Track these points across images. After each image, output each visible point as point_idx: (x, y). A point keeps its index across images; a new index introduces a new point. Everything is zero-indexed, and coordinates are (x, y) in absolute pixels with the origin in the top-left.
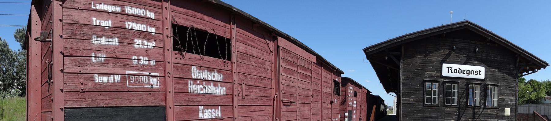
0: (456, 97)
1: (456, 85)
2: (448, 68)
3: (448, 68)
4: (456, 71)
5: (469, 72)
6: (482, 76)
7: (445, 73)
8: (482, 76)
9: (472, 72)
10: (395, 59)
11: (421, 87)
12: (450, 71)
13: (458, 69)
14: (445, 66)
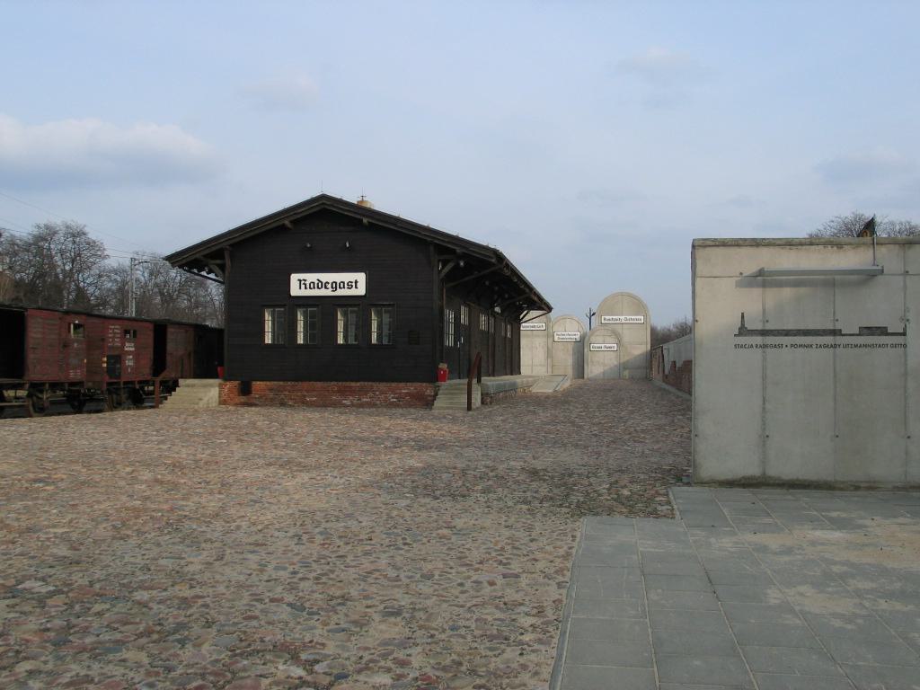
2: (300, 281)
3: (300, 281)
4: (312, 286)
5: (335, 286)
6: (361, 290)
7: (295, 291)
8: (361, 290)
9: (342, 285)
13: (316, 282)
14: (295, 278)
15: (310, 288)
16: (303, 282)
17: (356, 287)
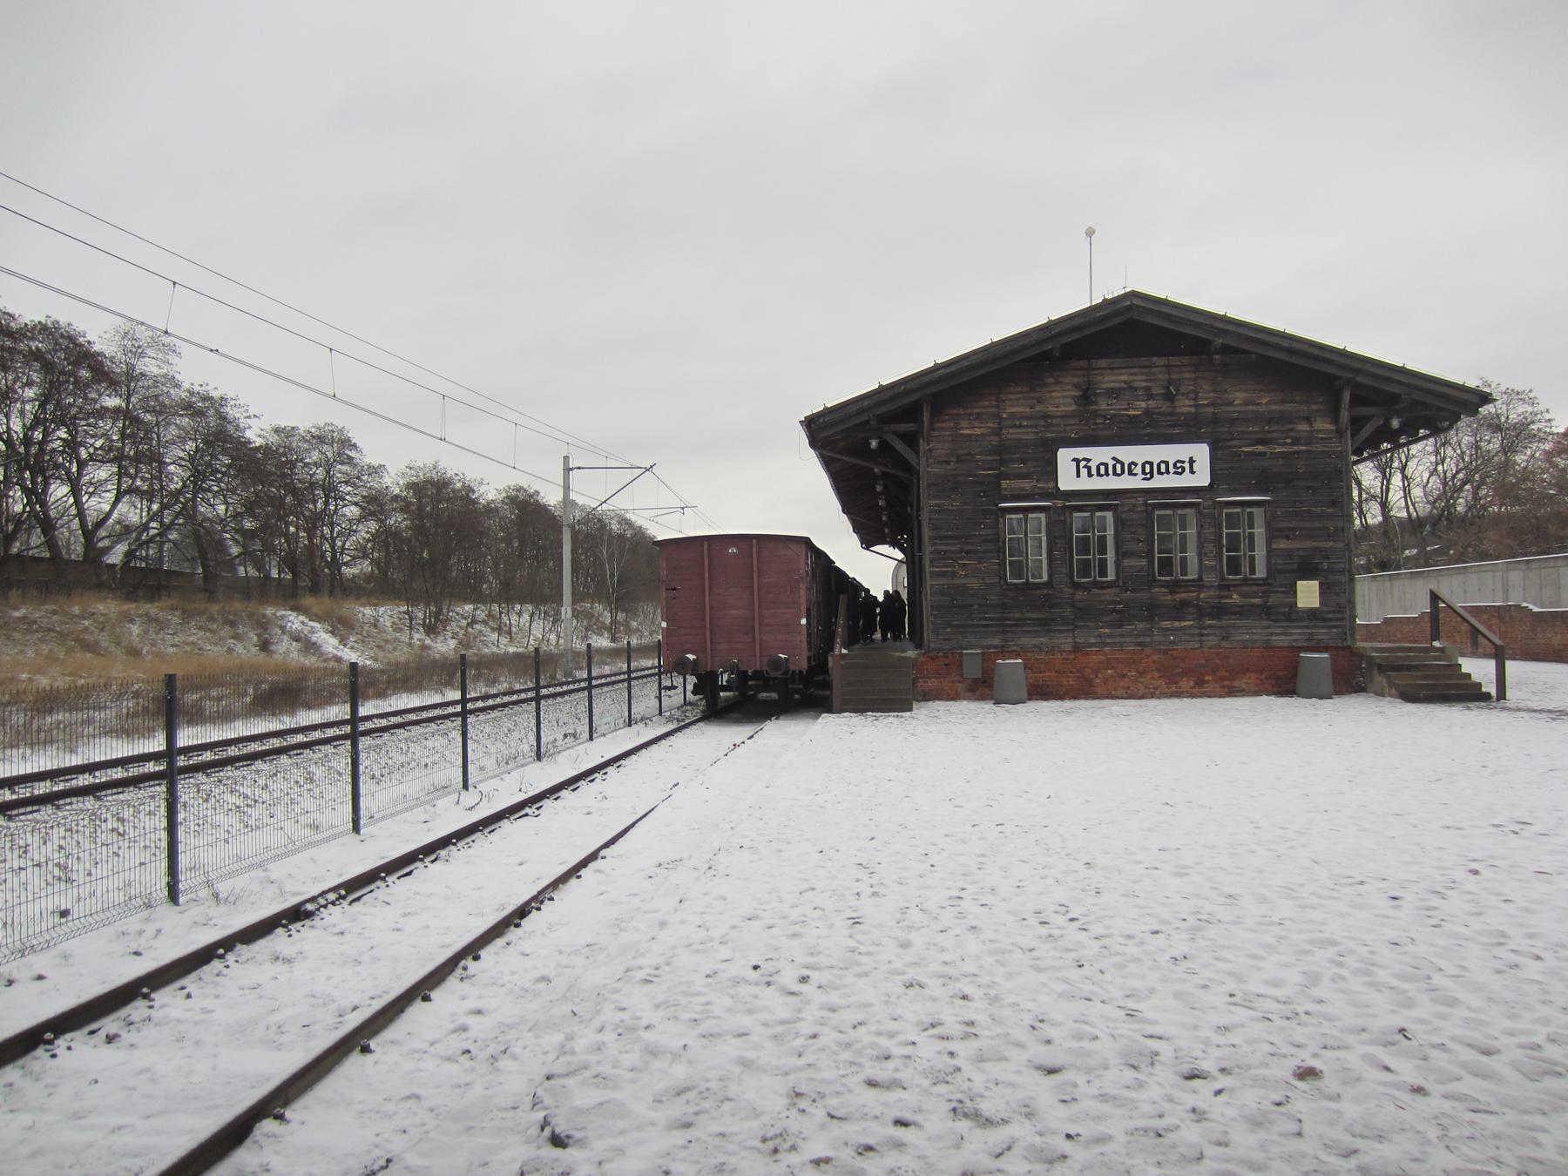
0: (1110, 556)
1: (1109, 515)
2: (1077, 461)
3: (1077, 461)
4: (1103, 470)
5: (1149, 470)
6: (1202, 478)
7: (1068, 480)
8: (1202, 478)
9: (1163, 468)
10: (900, 446)
11: (989, 531)
12: (1084, 472)
13: (1111, 463)
14: (1065, 456)
15: (1099, 474)
16: (1083, 464)
17: (1192, 472)
